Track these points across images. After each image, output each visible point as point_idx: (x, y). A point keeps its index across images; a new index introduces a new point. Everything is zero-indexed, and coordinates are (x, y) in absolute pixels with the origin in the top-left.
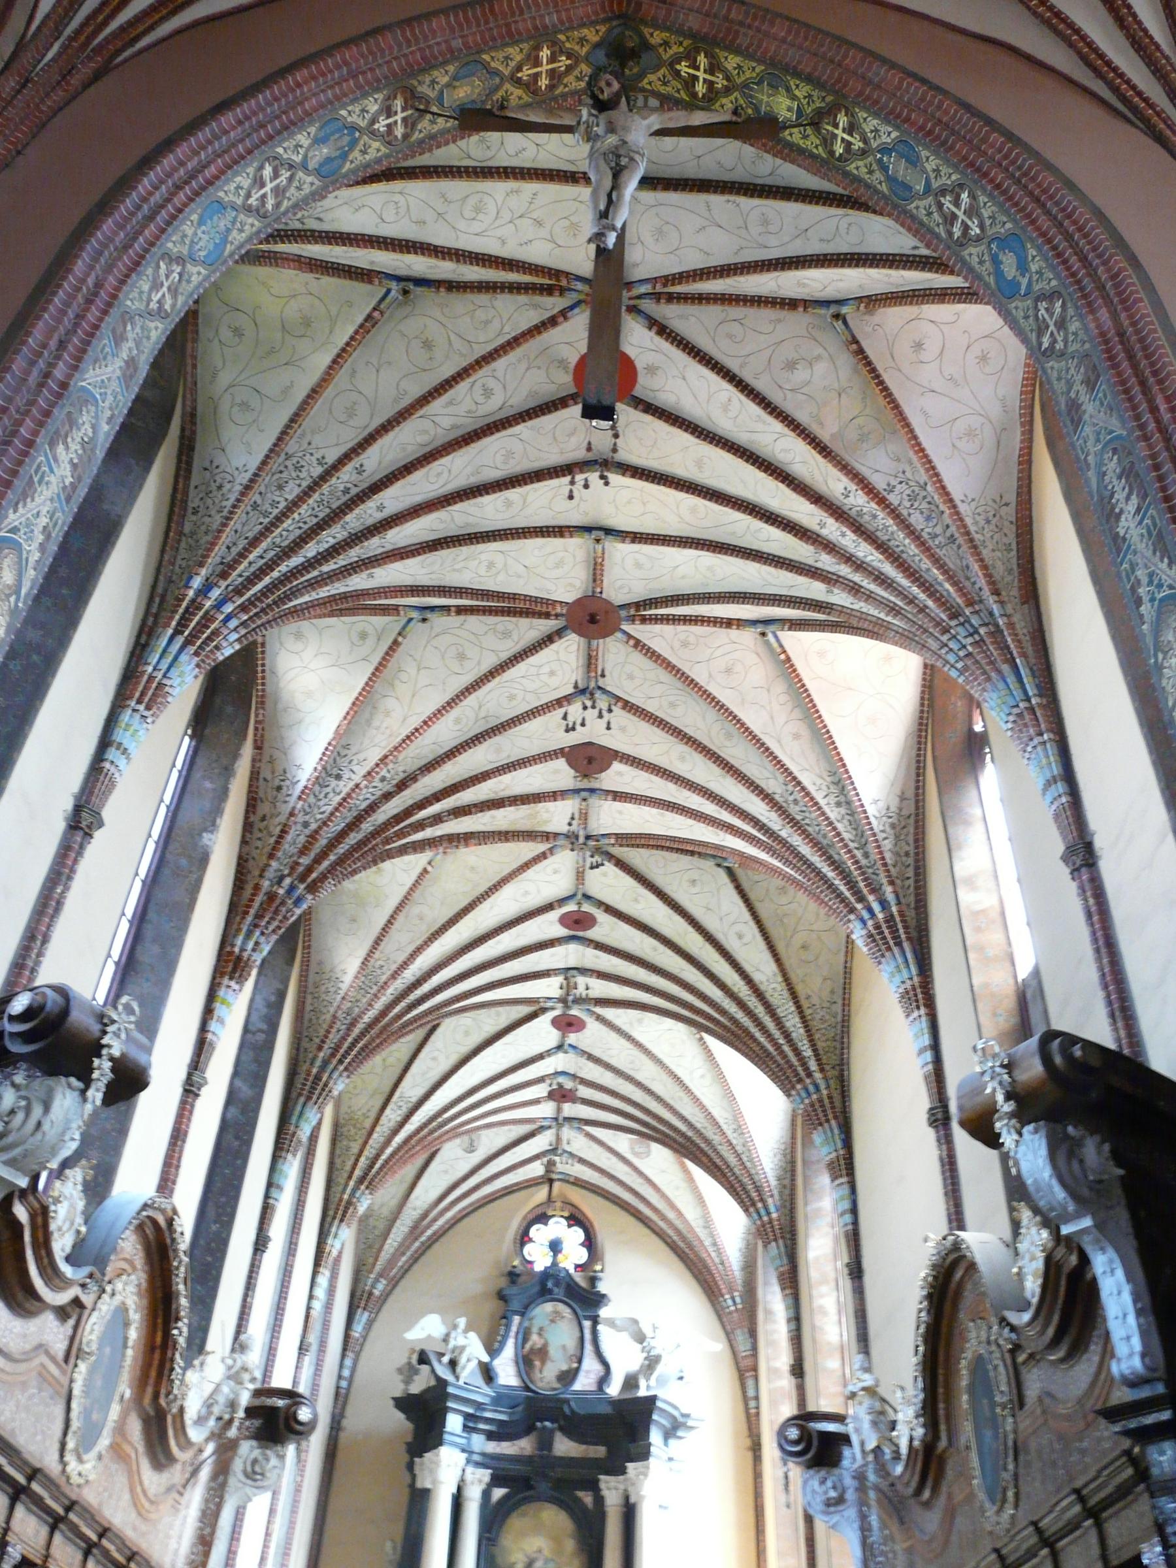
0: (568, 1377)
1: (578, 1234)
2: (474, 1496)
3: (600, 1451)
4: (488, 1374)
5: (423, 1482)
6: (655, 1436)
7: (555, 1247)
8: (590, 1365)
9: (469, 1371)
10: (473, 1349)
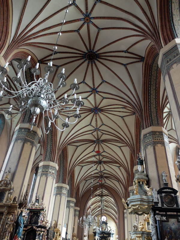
0: (105, 230)
1: (105, 217)
2: (99, 239)
3: (107, 236)
4: (99, 230)
5: (95, 238)
6: (111, 235)
7: (104, 219)
8: (107, 229)
9: (98, 230)
10: (98, 228)
